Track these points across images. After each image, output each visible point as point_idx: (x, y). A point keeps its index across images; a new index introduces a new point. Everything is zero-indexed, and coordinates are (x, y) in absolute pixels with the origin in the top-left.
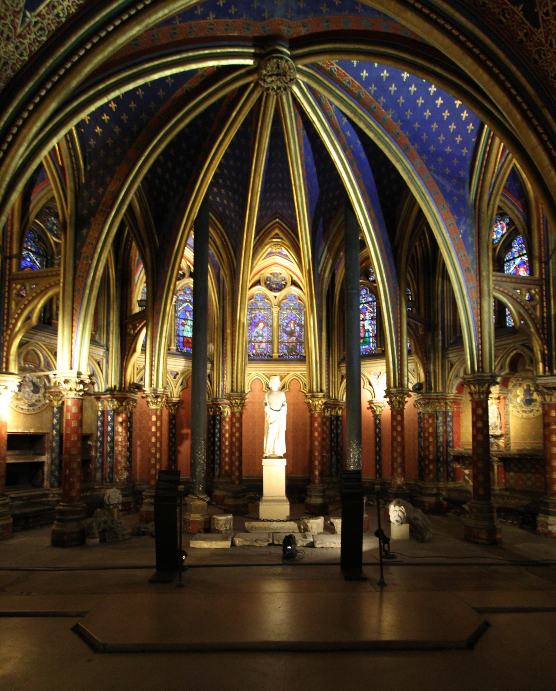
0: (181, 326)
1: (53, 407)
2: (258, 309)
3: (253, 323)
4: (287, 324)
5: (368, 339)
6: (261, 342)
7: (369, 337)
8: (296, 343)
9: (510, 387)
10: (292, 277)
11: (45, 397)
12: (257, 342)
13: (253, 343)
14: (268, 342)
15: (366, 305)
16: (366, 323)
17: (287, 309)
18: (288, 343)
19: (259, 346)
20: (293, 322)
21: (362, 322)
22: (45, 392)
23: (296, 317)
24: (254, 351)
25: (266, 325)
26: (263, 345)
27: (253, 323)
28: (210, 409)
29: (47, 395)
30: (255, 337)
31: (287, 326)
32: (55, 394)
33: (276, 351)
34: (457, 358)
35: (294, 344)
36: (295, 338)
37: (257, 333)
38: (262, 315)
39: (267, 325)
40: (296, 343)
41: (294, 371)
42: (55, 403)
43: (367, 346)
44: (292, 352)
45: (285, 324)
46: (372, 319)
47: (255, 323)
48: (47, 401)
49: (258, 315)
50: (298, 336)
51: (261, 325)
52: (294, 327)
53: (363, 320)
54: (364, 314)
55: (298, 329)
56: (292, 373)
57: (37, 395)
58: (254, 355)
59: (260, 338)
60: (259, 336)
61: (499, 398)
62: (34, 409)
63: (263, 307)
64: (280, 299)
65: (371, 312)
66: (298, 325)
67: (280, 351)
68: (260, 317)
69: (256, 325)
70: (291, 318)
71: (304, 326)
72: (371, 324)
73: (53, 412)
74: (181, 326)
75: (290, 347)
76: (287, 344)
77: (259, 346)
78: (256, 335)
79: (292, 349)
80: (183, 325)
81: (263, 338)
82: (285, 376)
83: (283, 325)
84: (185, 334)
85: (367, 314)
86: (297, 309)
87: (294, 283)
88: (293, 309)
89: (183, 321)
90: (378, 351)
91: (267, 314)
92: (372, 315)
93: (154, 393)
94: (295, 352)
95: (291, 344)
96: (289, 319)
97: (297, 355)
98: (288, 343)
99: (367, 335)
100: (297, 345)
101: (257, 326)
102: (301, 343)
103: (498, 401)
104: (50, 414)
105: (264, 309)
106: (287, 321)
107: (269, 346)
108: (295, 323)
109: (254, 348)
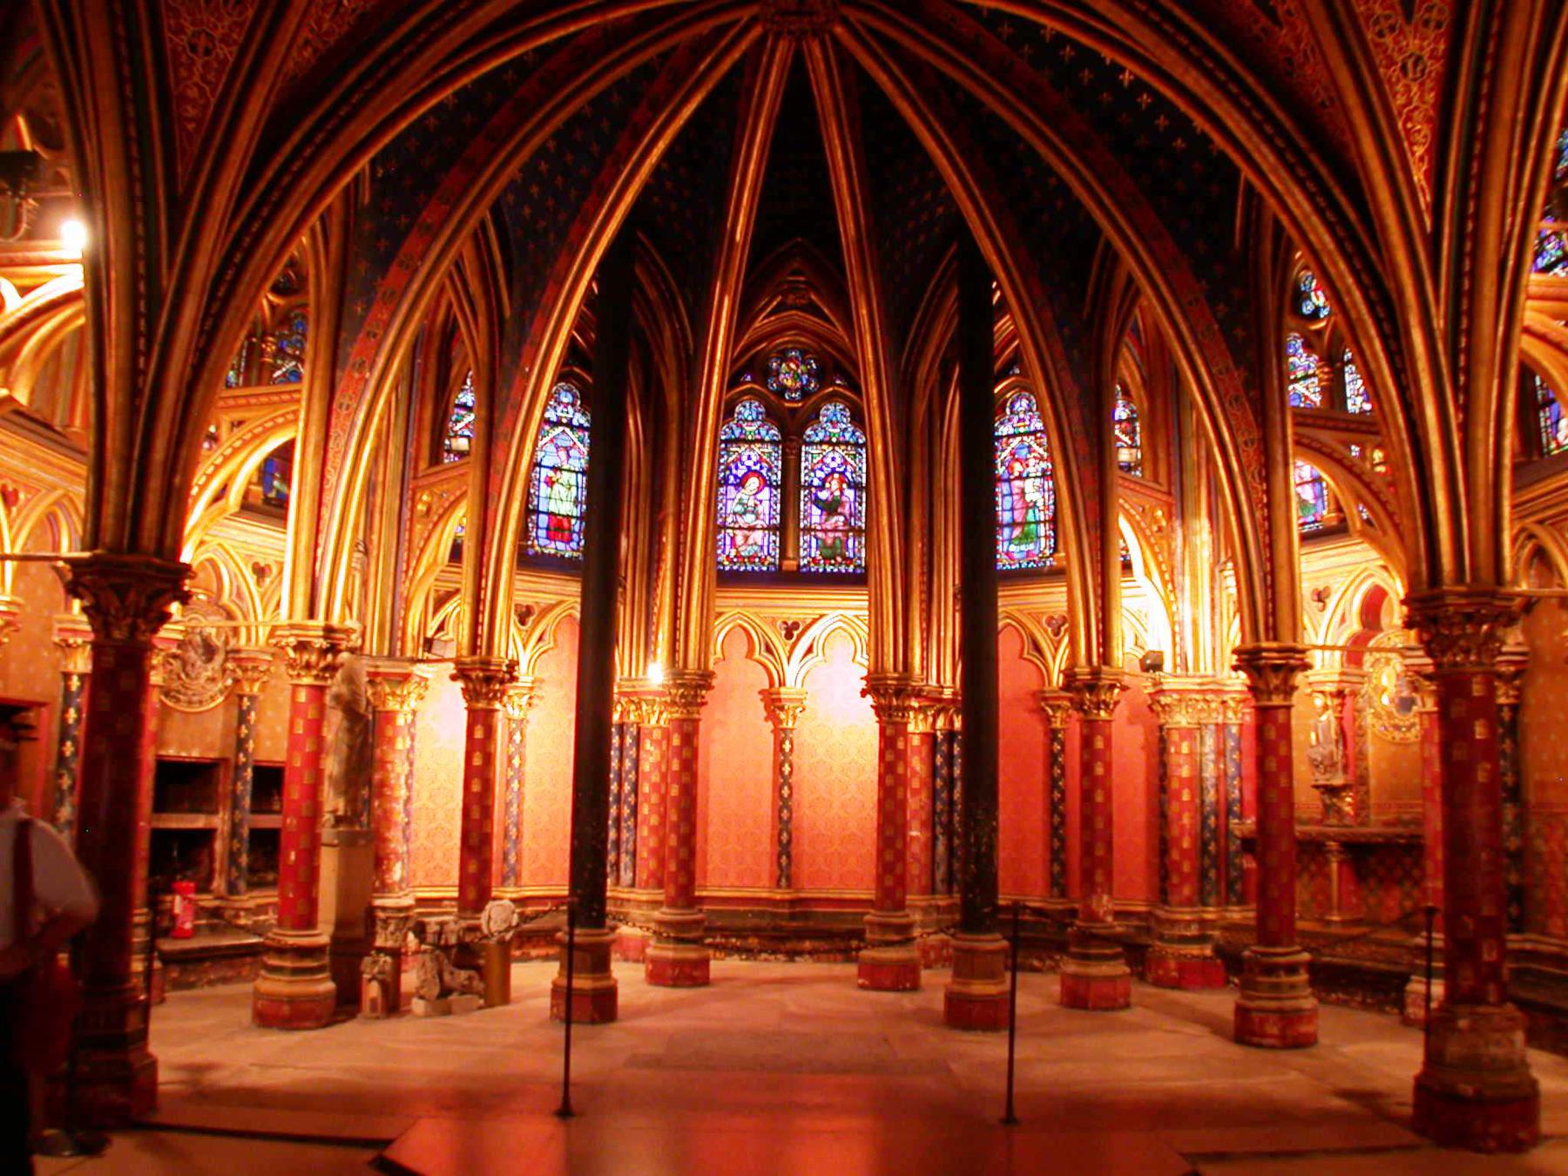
0: (543, 486)
2: (746, 441)
3: (732, 479)
4: (824, 481)
5: (1033, 526)
6: (752, 529)
7: (1038, 523)
8: (845, 532)
9: (1367, 668)
11: (224, 670)
12: (740, 528)
14: (770, 528)
15: (1029, 440)
17: (821, 443)
19: (747, 538)
21: (1017, 483)
23: (845, 462)
25: (766, 483)
26: (757, 536)
27: (732, 479)
29: (230, 665)
31: (821, 488)
33: (790, 554)
36: (842, 519)
37: (740, 503)
38: (755, 459)
39: (770, 486)
40: (845, 532)
43: (1031, 547)
45: (816, 482)
46: (1044, 476)
47: (736, 477)
48: (229, 682)
49: (744, 458)
51: (753, 482)
52: (842, 490)
53: (1020, 478)
54: (1024, 462)
55: (850, 493)
56: (832, 614)
58: (731, 561)
59: (749, 518)
60: (745, 513)
61: (1340, 694)
65: (1041, 459)
66: (855, 486)
67: (802, 553)
69: (741, 483)
71: (867, 488)
74: (543, 486)
75: (829, 542)
76: (820, 535)
77: (747, 538)
78: (739, 508)
79: (832, 547)
80: (550, 483)
82: (814, 621)
83: (811, 485)
84: (553, 508)
85: (1032, 462)
86: (847, 443)
88: (838, 444)
89: (551, 473)
90: (1058, 560)
92: (1043, 465)
93: (482, 670)
95: (831, 535)
96: (828, 470)
99: (1030, 517)
102: (858, 532)
103: (1337, 701)
105: (762, 441)
106: (821, 474)
108: (841, 481)
109: (733, 544)
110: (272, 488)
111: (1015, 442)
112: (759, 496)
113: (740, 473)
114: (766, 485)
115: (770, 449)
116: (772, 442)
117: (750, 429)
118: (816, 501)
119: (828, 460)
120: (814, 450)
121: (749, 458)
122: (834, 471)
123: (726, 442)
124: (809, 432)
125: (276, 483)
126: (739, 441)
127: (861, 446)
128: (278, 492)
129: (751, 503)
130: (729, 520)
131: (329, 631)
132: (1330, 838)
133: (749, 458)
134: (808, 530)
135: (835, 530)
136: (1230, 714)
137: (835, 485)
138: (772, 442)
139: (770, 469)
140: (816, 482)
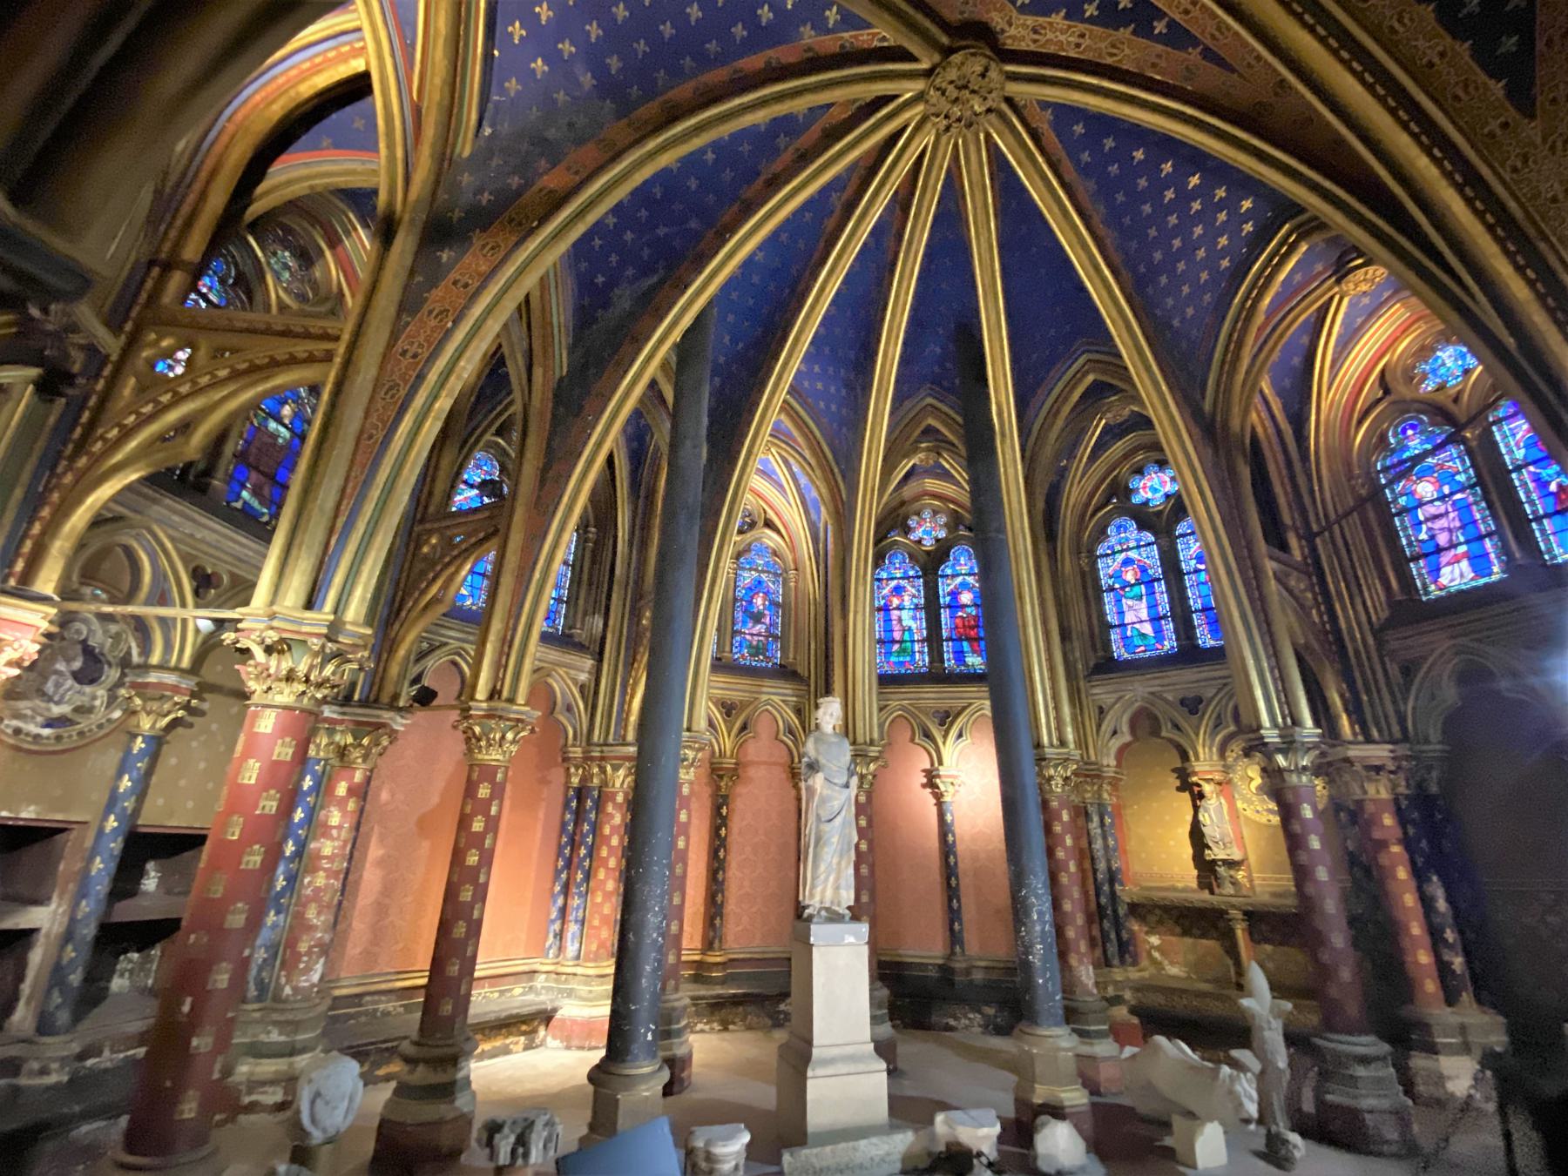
1: (135, 736)
11: (112, 700)
16: (905, 615)
22: (120, 684)
28: (572, 770)
29: (123, 692)
32: (157, 693)
34: (1116, 696)
42: (146, 723)
46: (917, 608)
57: (88, 689)
62: (58, 738)
72: (914, 618)
73: (128, 750)
79: (757, 647)
87: (769, 524)
104: (113, 757)
110: (239, 497)
111: (893, 583)
125: (245, 494)
128: (245, 503)
131: (335, 628)
132: (1234, 907)
136: (1105, 796)
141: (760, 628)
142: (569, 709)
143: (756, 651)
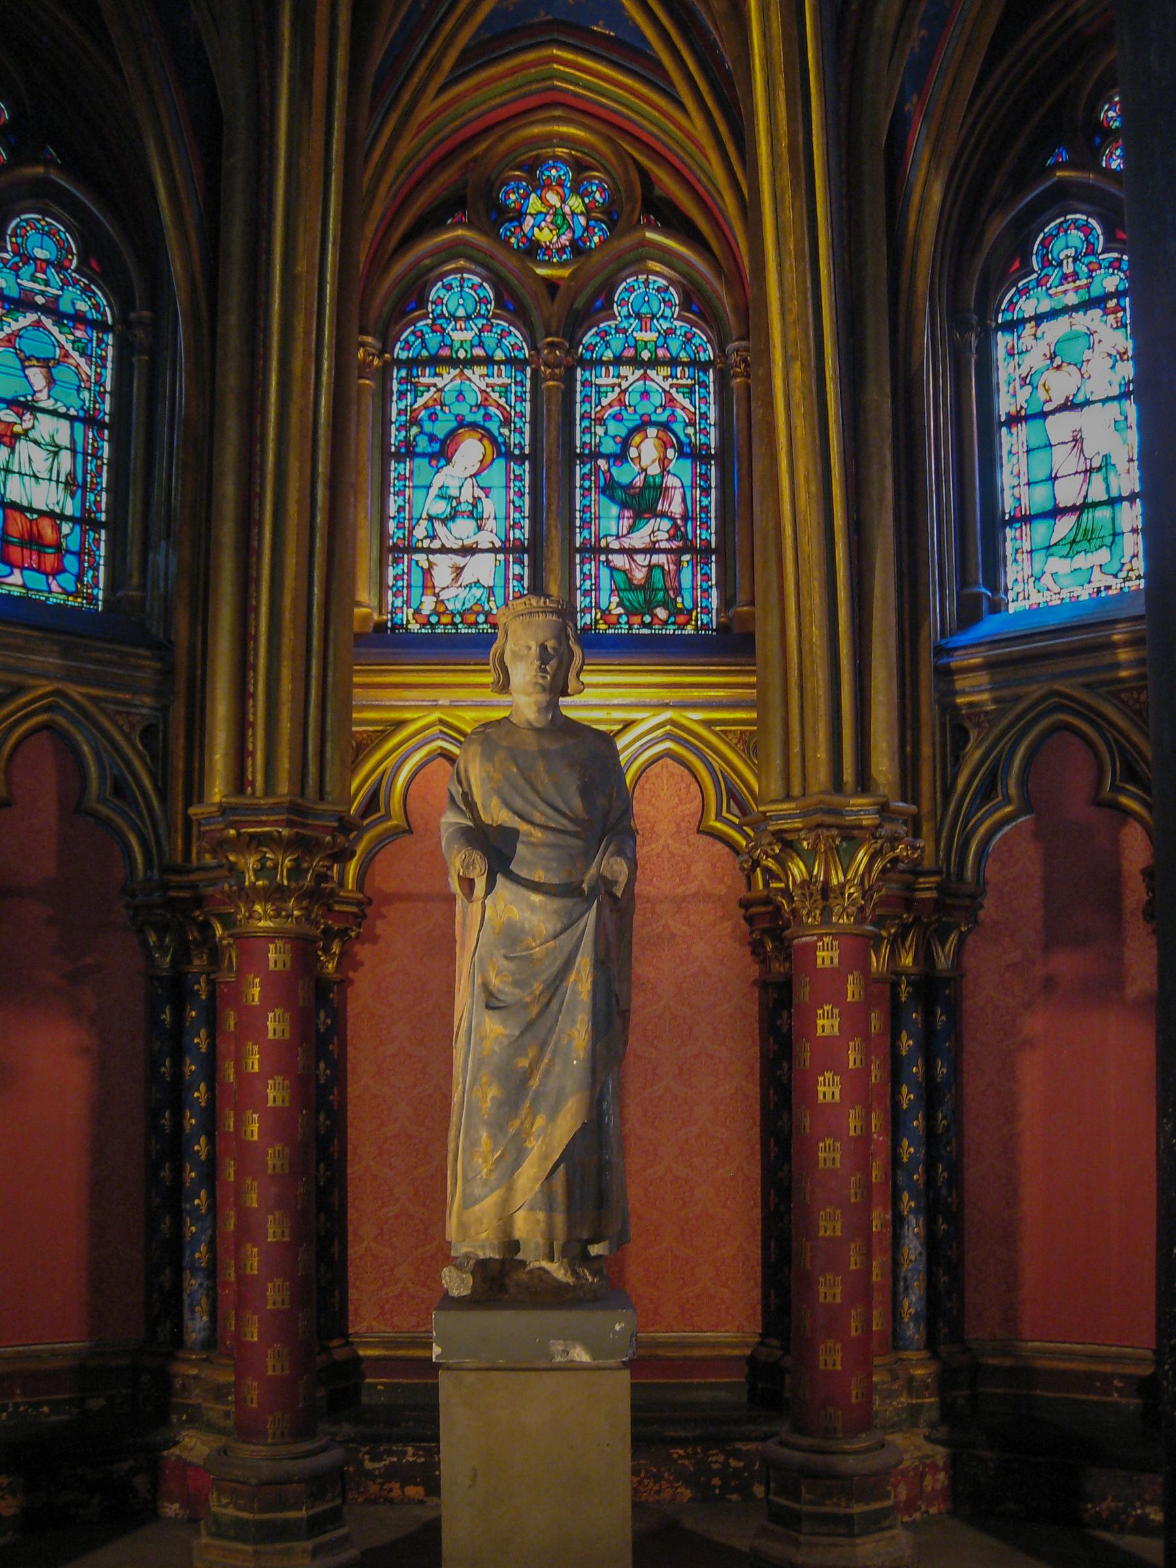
2: (453, 362)
6: (468, 551)
10: (644, 173)
12: (444, 550)
13: (421, 558)
18: (622, 551)
20: (652, 432)
24: (428, 604)
27: (423, 445)
28: (152, 939)
30: (430, 518)
31: (621, 457)
35: (661, 559)
36: (666, 524)
38: (472, 398)
39: (508, 456)
41: (666, 706)
44: (649, 607)
47: (432, 438)
49: (449, 398)
50: (685, 517)
51: (471, 450)
52: (664, 462)
55: (682, 469)
60: (452, 517)
63: (479, 352)
64: (579, 303)
67: (581, 601)
68: (462, 409)
69: (444, 452)
70: (645, 408)
75: (639, 575)
76: (619, 560)
78: (440, 508)
79: (646, 587)
81: (480, 528)
83: (596, 455)
91: (506, 387)
94: (664, 604)
95: (639, 558)
97: (682, 626)
98: (622, 551)
100: (678, 564)
101: (449, 461)
102: (703, 553)
105: (488, 361)
107: (517, 569)
112: (483, 480)
113: (441, 429)
114: (499, 455)
115: (504, 376)
116: (510, 361)
117: (461, 336)
118: (609, 488)
119: (632, 398)
120: (603, 379)
121: (460, 397)
122: (645, 424)
123: (411, 363)
124: (588, 339)
126: (435, 361)
127: (704, 367)
129: (466, 495)
130: (420, 532)
133: (460, 397)
134: (594, 550)
135: (652, 550)
137: (648, 450)
138: (510, 361)
139: (507, 422)
140: (609, 447)
141: (655, 530)
142: (119, 789)
143: (645, 595)
